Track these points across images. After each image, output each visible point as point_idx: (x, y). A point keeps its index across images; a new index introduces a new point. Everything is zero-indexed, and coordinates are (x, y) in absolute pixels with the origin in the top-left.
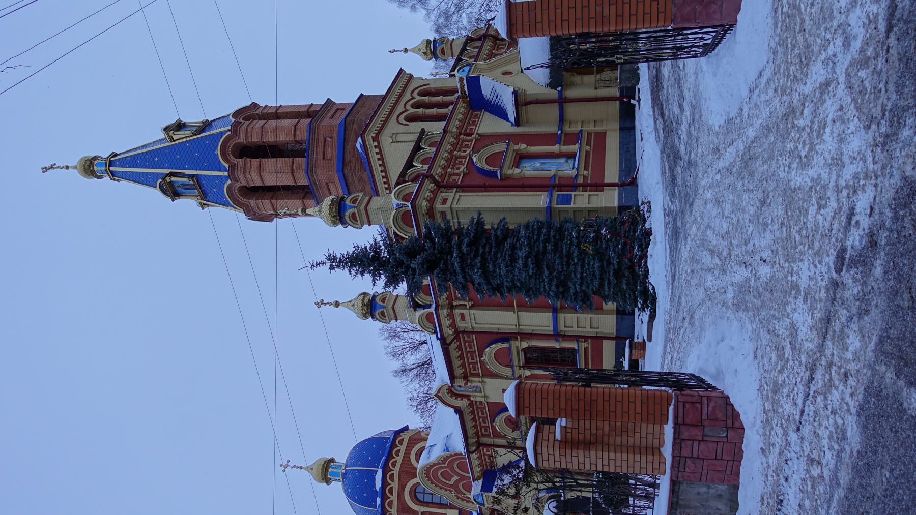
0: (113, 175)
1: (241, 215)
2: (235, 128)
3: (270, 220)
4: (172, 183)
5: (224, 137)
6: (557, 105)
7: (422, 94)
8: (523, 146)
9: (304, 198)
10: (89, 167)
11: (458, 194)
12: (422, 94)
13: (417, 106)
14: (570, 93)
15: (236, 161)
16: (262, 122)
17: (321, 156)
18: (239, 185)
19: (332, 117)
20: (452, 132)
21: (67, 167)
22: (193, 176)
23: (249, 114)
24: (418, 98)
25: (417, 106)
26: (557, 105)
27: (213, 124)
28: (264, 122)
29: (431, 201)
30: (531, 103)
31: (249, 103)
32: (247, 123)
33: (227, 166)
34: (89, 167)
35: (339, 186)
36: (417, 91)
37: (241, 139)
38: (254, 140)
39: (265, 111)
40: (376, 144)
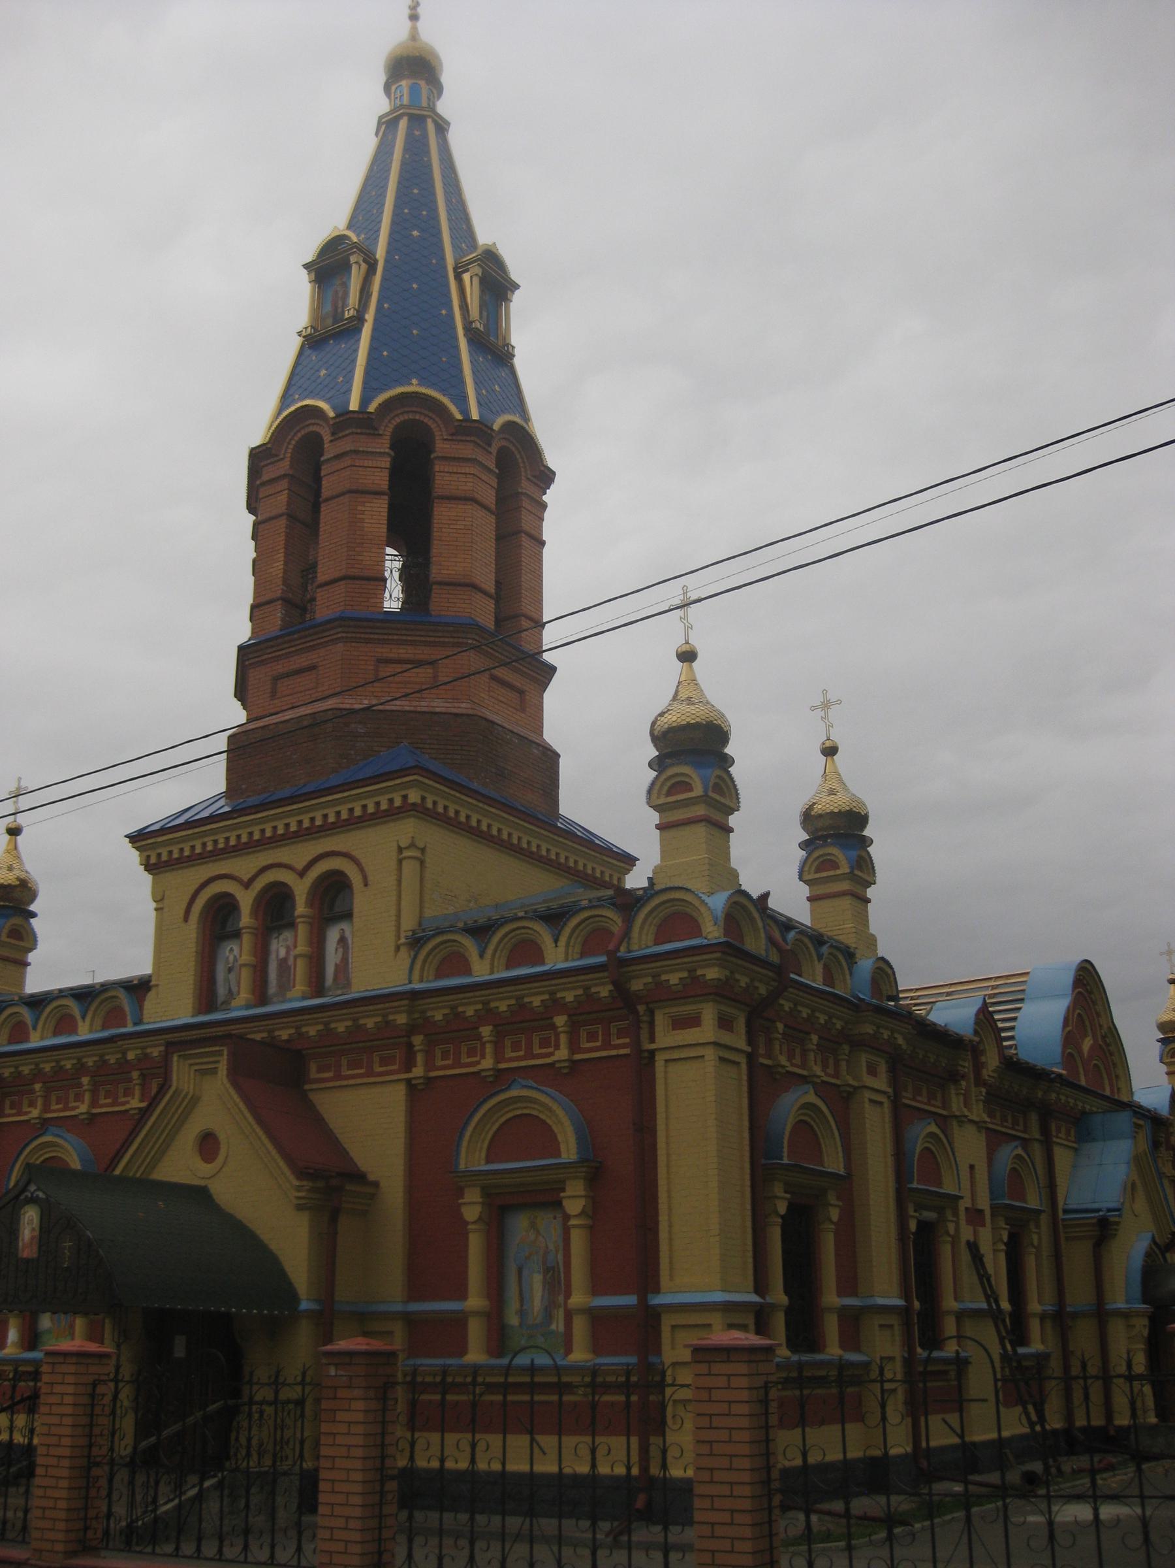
0: (387, 124)
1: (258, 435)
2: (476, 431)
3: (251, 508)
4: (346, 267)
5: (445, 400)
9: (285, 600)
10: (414, 70)
15: (387, 429)
16: (489, 496)
18: (327, 438)
21: (414, 17)
22: (360, 319)
23: (519, 470)
27: (504, 373)
28: (493, 507)
31: (552, 460)
33: (372, 408)
34: (414, 70)
37: (441, 447)
39: (526, 503)
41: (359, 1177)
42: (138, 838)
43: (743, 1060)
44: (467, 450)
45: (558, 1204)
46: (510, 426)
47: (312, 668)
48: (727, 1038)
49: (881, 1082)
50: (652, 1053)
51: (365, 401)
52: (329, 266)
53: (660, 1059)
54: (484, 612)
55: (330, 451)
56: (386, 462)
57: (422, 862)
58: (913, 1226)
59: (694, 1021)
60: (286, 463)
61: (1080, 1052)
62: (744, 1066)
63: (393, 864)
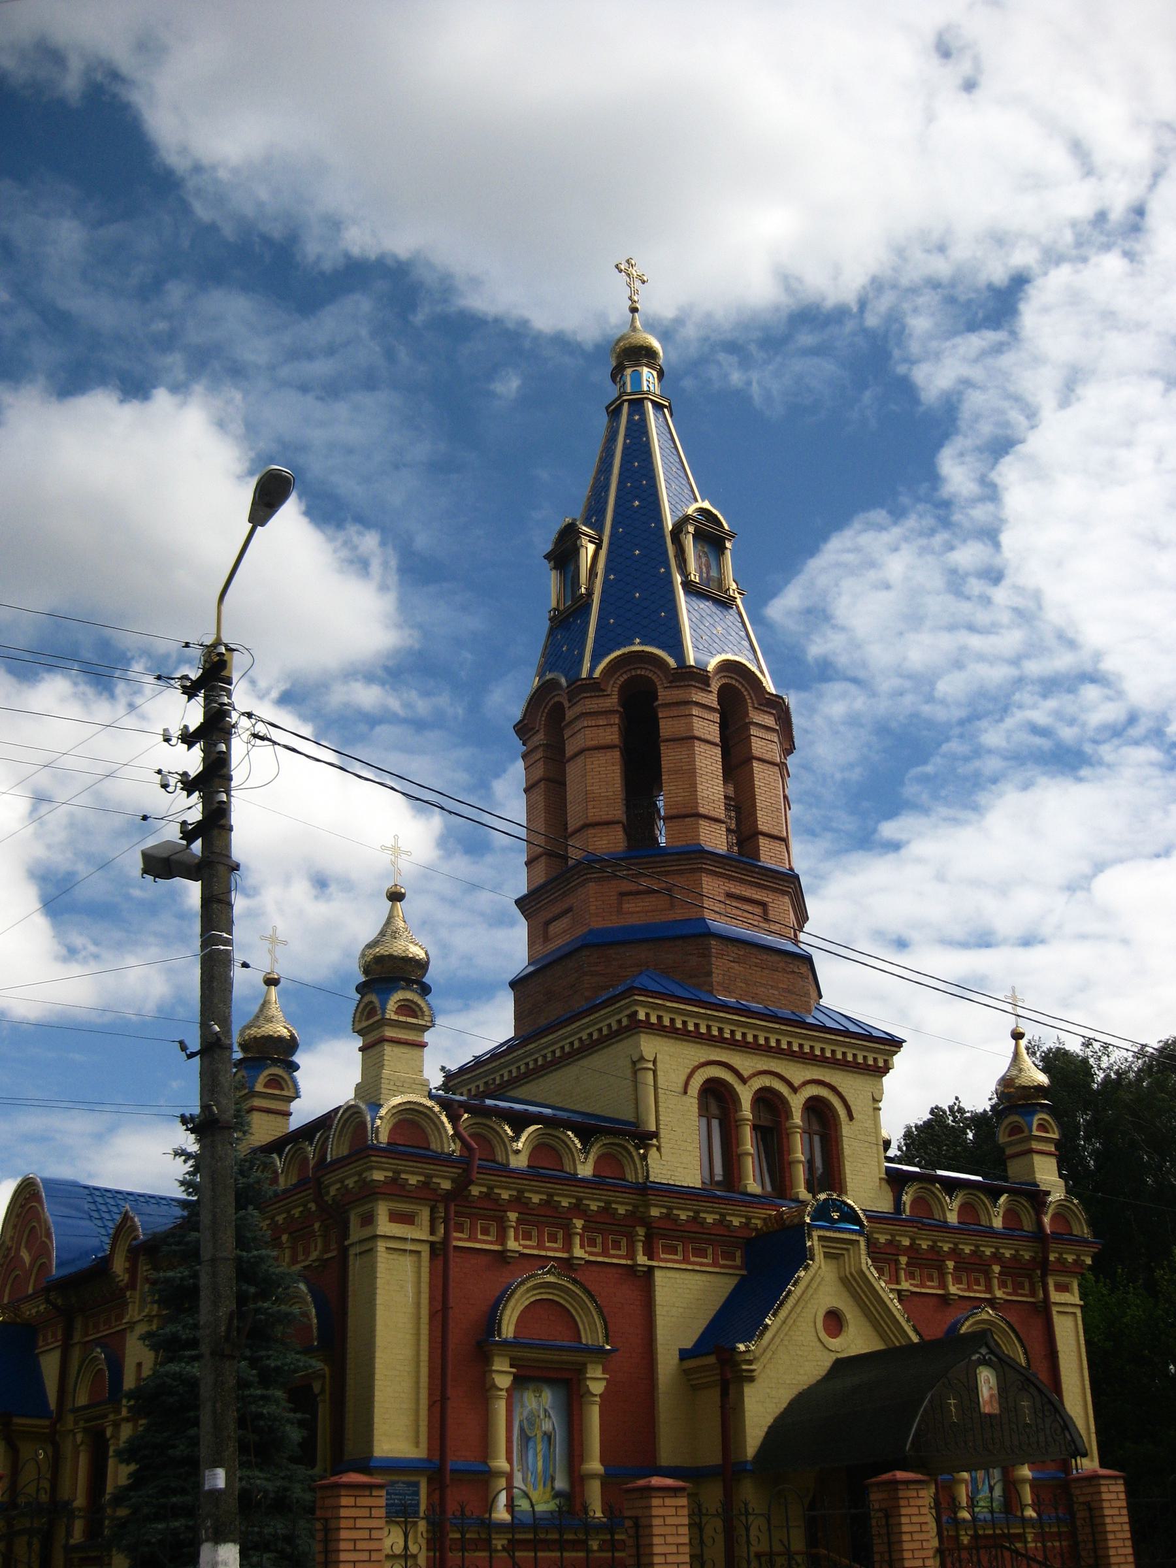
6: (715, 1459)
7: (818, 1110)
8: (597, 1388)
11: (425, 1250)
12: (818, 1110)
13: (768, 1101)
14: (748, 1492)
17: (627, 886)
18: (566, 704)
19: (730, 895)
20: (648, 1206)
22: (590, 593)
24: (797, 1103)
25: (768, 1101)
26: (715, 1459)
28: (718, 740)
29: (395, 1189)
30: (725, 1393)
32: (712, 700)
33: (597, 674)
35: (567, 938)
36: (824, 1092)
37: (664, 695)
38: (662, 723)
40: (625, 1022)
46: (728, 667)
47: (569, 910)
51: (592, 669)
52: (563, 554)
54: (716, 839)
55: (570, 714)
57: (655, 1072)
60: (542, 732)
63: (628, 1073)
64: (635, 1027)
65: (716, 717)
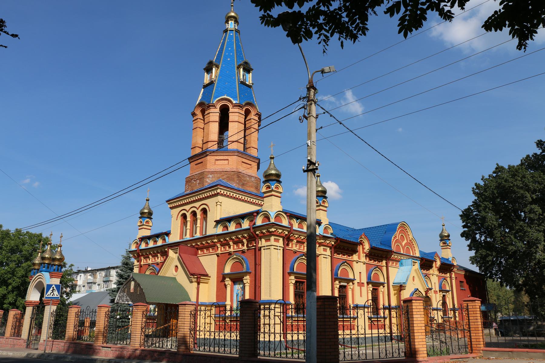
15: (218, 106)
32: (243, 113)
37: (231, 110)
41: (207, 275)
42: (167, 201)
43: (282, 249)
44: (236, 110)
45: (242, 281)
48: (276, 244)
49: (328, 252)
50: (261, 247)
53: (262, 248)
56: (218, 114)
58: (338, 286)
59: (269, 240)
61: (402, 245)
62: (282, 250)
64: (217, 194)
65: (244, 117)
